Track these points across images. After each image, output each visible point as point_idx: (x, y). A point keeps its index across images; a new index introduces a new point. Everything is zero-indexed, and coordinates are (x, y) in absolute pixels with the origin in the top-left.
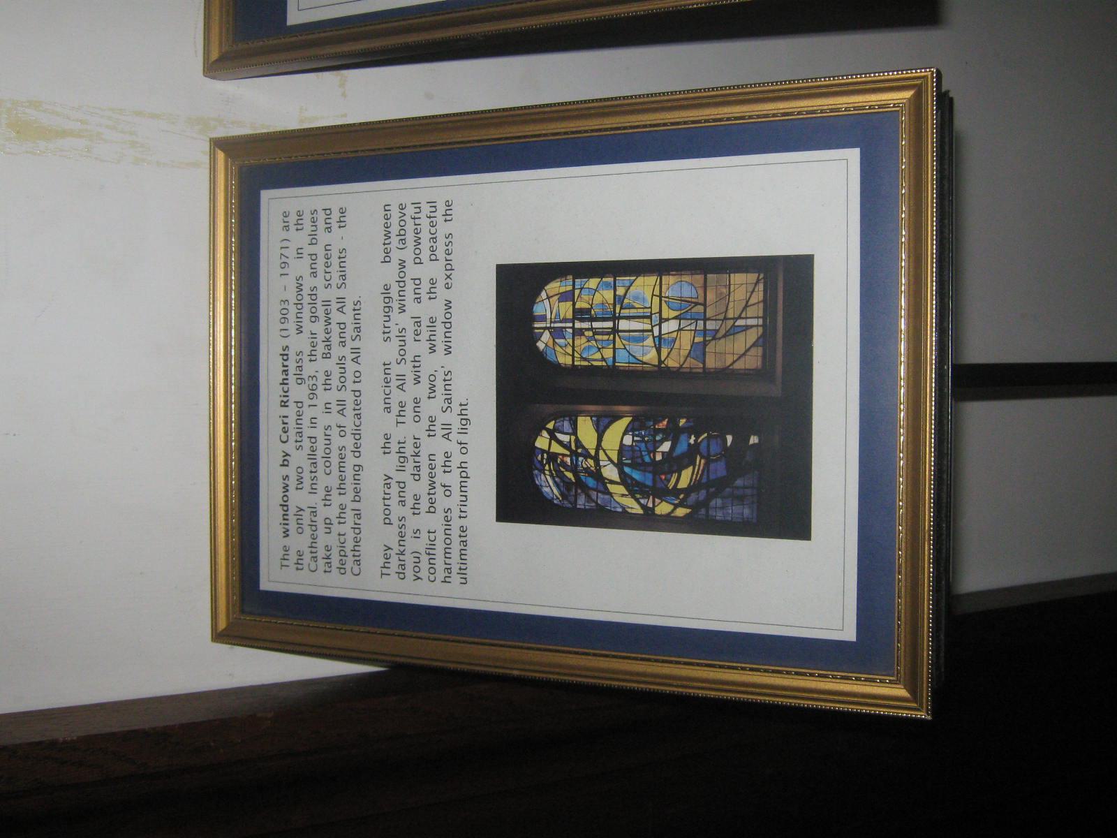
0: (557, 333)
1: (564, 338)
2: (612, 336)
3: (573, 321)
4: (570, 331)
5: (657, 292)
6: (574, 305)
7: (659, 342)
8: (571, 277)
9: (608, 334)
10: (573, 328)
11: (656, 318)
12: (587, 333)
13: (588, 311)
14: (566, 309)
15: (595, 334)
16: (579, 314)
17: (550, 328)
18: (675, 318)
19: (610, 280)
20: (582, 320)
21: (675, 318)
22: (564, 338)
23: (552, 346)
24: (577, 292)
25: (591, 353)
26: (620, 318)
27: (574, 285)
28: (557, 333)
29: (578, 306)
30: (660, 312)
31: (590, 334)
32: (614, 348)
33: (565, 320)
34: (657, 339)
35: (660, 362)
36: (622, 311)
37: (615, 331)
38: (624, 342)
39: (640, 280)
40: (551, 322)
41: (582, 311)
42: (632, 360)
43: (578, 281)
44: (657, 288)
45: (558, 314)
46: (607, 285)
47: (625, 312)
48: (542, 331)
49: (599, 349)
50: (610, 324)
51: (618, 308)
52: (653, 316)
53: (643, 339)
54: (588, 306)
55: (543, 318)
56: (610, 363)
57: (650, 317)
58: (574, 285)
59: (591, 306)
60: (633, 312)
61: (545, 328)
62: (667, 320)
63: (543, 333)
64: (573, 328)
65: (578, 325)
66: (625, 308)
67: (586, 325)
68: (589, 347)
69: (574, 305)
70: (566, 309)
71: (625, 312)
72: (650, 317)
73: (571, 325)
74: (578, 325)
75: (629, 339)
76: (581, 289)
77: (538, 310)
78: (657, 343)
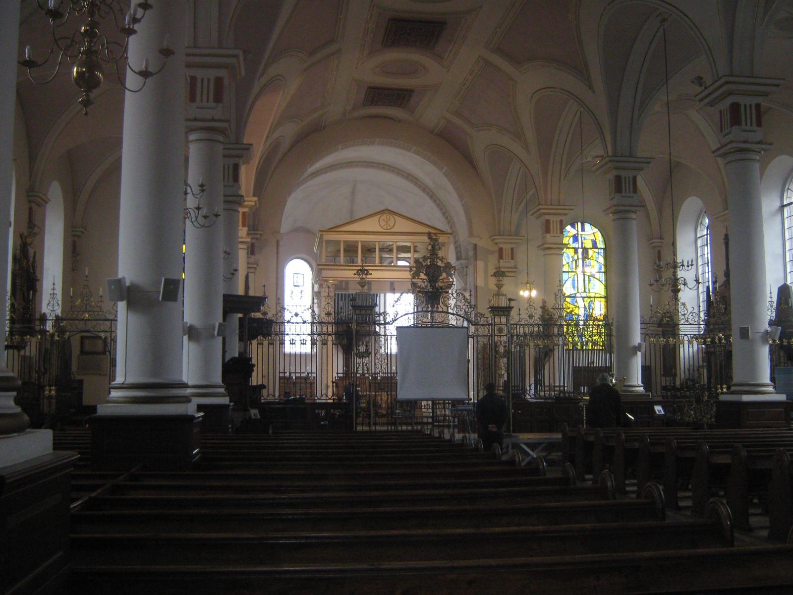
0: (575, 238)
1: (573, 243)
3: (582, 248)
4: (577, 247)
5: (597, 295)
6: (590, 249)
7: (573, 297)
8: (604, 247)
10: (578, 248)
11: (584, 295)
12: (576, 256)
14: (588, 244)
15: (576, 261)
16: (585, 251)
17: (578, 234)
18: (585, 305)
19: (603, 270)
21: (585, 305)
22: (573, 243)
23: (569, 235)
24: (596, 250)
25: (566, 258)
27: (601, 249)
28: (575, 238)
29: (589, 250)
31: (576, 258)
32: (568, 272)
33: (582, 243)
34: (574, 295)
36: (587, 276)
38: (572, 277)
39: (603, 287)
40: (581, 235)
41: (587, 253)
42: (564, 282)
43: (602, 251)
44: (599, 296)
46: (600, 268)
48: (576, 229)
49: (568, 263)
52: (585, 293)
53: (574, 288)
54: (590, 257)
55: (583, 230)
57: (585, 291)
58: (601, 249)
59: (590, 259)
60: (587, 282)
61: (578, 231)
62: (584, 301)
63: (575, 229)
64: (578, 248)
65: (580, 251)
66: (589, 278)
67: (580, 256)
68: (569, 257)
69: (590, 249)
70: (588, 244)
72: (585, 291)
73: (580, 247)
74: (580, 251)
75: (574, 280)
76: (598, 253)
77: (587, 226)
78: (572, 295)
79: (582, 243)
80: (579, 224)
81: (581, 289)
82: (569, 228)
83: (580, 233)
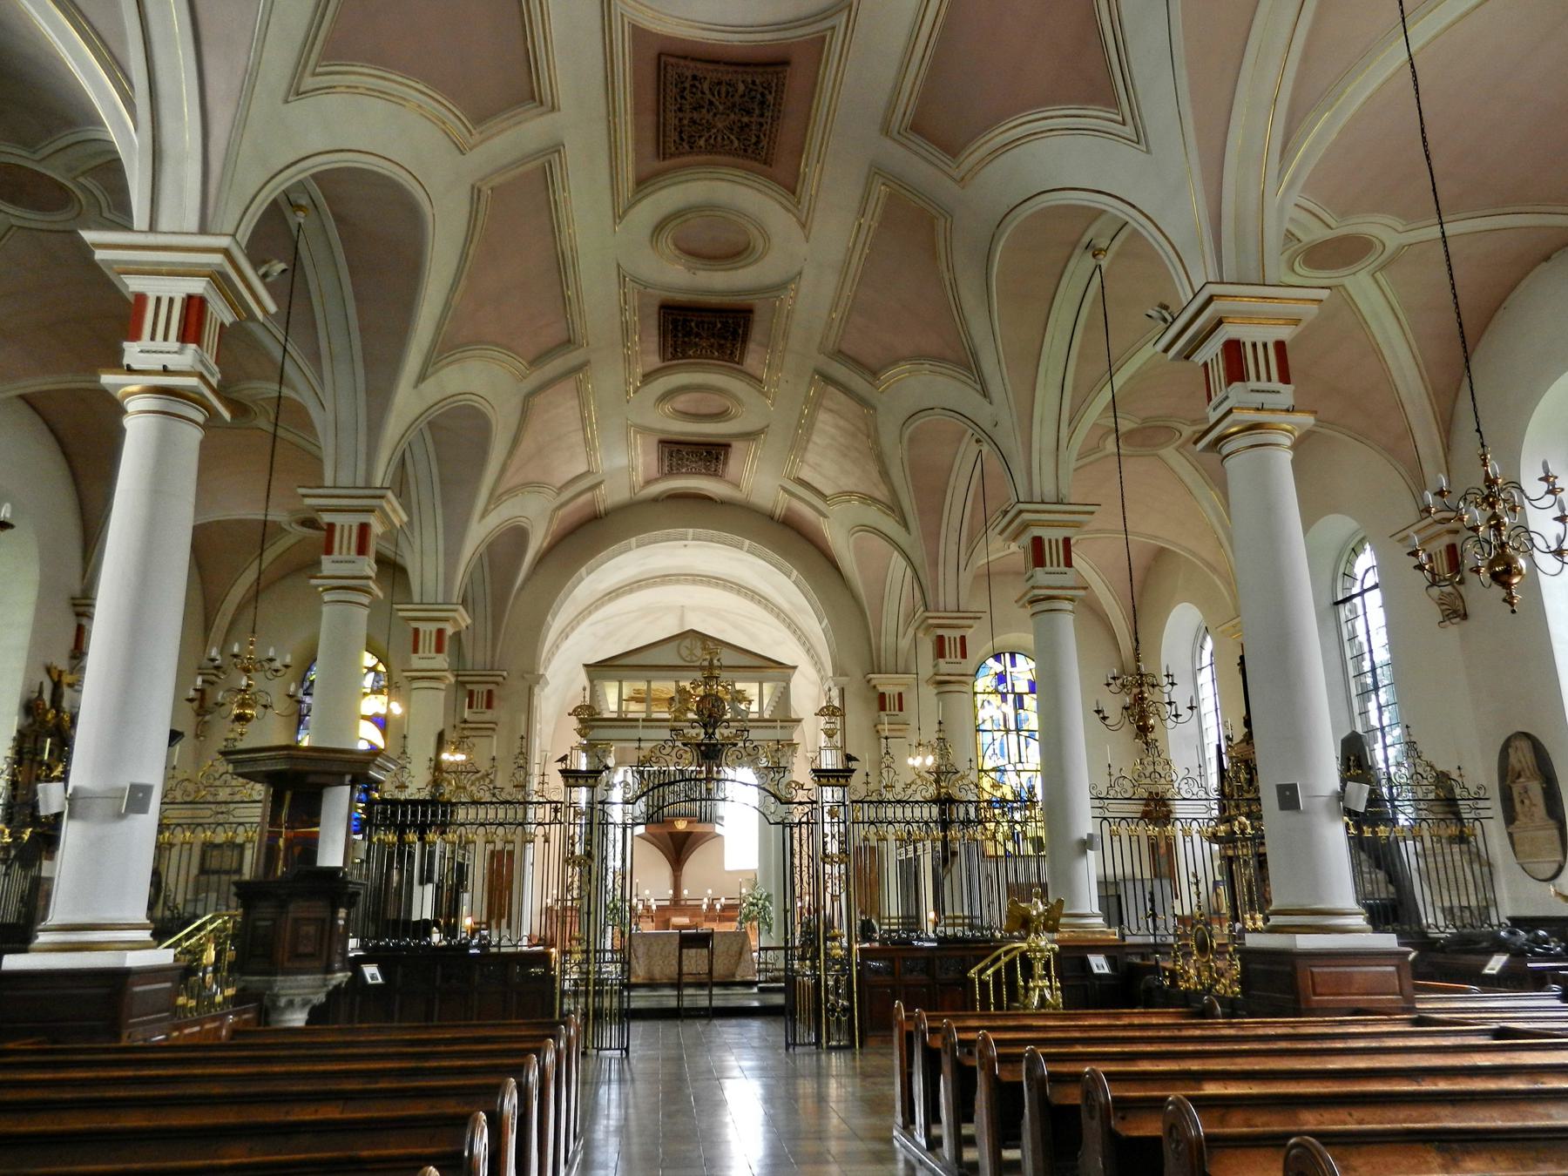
0: (1001, 678)
2: (1002, 728)
3: (1013, 692)
4: (1005, 691)
9: (1005, 726)
10: (1008, 692)
11: (1019, 767)
13: (1022, 707)
16: (1019, 698)
20: (1015, 699)
26: (1019, 735)
30: (1024, 771)
33: (1013, 685)
35: (985, 771)
37: (1008, 731)
45: (1018, 679)
47: (1022, 739)
50: (1012, 727)
51: (1027, 734)
55: (1013, 664)
56: (982, 727)
57: (1020, 762)
65: (1010, 697)
71: (1022, 739)
72: (1020, 762)
74: (1010, 697)
79: (1013, 685)
80: (1007, 655)
81: (1015, 758)
82: (991, 662)
83: (1009, 669)
